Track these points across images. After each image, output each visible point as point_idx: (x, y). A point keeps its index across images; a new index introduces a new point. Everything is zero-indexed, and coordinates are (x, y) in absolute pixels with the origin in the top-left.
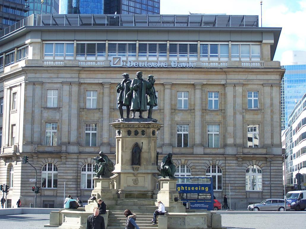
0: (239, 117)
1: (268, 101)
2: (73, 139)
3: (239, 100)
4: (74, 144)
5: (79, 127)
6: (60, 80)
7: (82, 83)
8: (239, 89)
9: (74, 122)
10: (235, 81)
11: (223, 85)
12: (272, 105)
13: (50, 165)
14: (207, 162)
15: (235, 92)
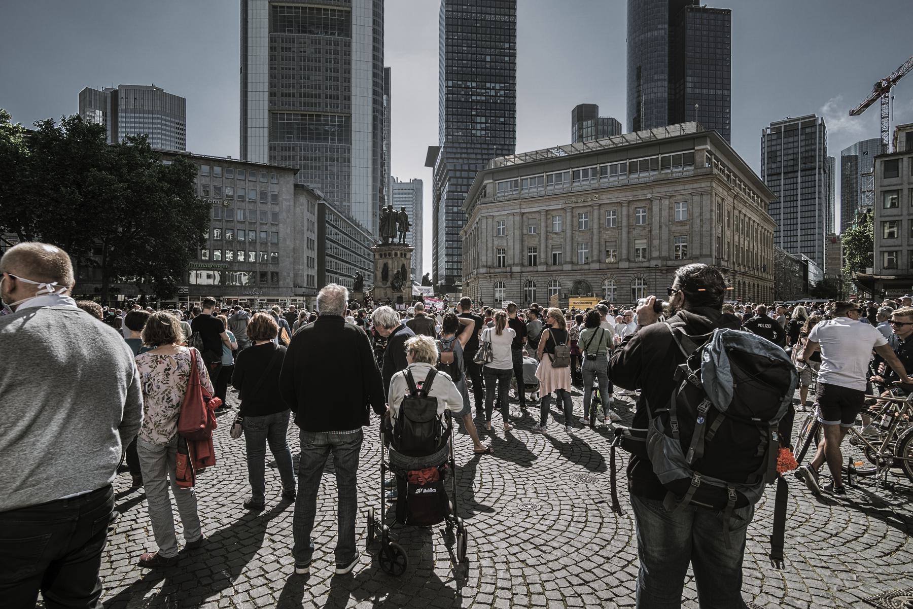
0: (665, 230)
1: (697, 211)
2: (517, 261)
3: (665, 213)
4: (517, 265)
5: (522, 251)
6: (506, 212)
7: (524, 213)
8: (667, 202)
9: (518, 247)
10: (660, 194)
11: (649, 199)
12: (701, 214)
13: (501, 283)
14: (632, 275)
15: (661, 205)
